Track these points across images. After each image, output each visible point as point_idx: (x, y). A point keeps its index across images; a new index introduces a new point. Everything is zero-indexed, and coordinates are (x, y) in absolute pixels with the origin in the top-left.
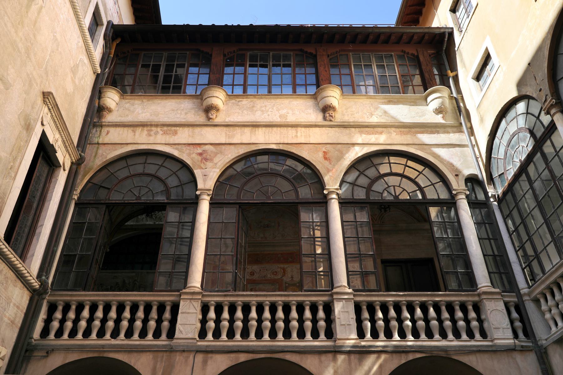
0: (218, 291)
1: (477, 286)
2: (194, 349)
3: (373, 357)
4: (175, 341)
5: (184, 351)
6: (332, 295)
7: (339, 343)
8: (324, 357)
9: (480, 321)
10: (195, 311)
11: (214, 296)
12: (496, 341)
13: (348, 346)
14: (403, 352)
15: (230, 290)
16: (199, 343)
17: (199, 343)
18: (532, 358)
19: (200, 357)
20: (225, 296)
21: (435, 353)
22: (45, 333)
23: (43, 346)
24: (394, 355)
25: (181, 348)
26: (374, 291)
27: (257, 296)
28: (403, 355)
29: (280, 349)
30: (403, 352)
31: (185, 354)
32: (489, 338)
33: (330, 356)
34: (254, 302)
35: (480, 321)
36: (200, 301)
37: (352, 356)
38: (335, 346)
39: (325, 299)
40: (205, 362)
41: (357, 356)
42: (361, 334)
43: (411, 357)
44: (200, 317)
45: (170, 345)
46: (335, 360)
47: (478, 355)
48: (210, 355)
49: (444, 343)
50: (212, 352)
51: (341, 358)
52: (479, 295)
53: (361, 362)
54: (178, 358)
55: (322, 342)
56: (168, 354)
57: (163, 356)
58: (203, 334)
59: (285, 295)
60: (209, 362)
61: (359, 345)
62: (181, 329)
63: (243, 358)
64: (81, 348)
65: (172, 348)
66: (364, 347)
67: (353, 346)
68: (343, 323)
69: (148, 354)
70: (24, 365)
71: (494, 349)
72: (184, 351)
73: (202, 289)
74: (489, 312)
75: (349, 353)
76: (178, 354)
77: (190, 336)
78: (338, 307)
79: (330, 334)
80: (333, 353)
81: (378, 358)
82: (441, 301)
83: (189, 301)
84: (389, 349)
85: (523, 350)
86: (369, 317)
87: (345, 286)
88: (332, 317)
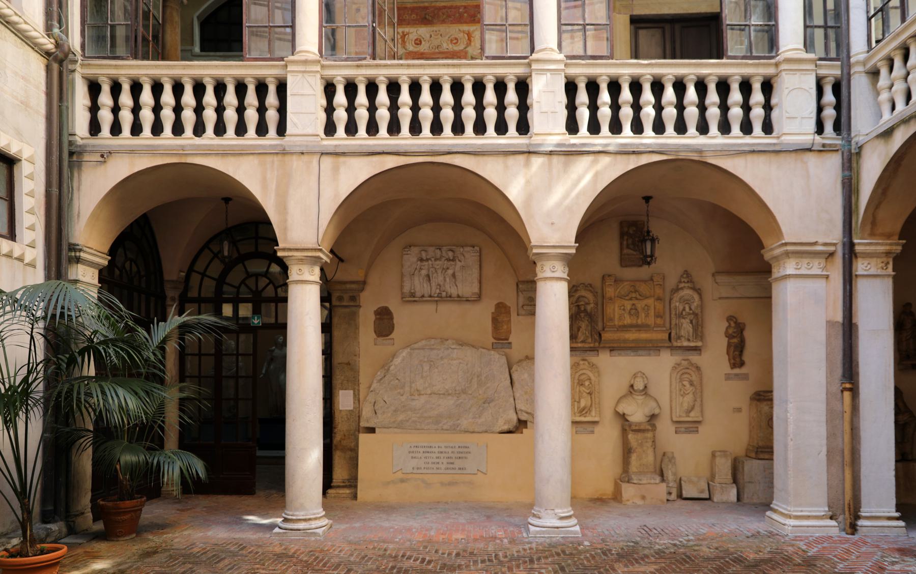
0: (346, 60)
1: (778, 49)
2: (317, 149)
3: (587, 159)
4: (287, 139)
5: (303, 153)
6: (529, 65)
7: (536, 140)
8: (511, 160)
9: (768, 107)
10: (312, 92)
11: (340, 67)
12: (783, 138)
13: (549, 145)
14: (634, 153)
15: (365, 59)
16: (325, 143)
17: (325, 143)
18: (834, 162)
19: (327, 161)
20: (358, 66)
21: (683, 155)
22: (95, 128)
23: (94, 146)
24: (619, 157)
25: (298, 149)
26: (601, 57)
27: (409, 66)
28: (633, 157)
29: (446, 149)
30: (634, 153)
31: (305, 158)
32: (774, 134)
33: (521, 158)
34: (405, 78)
35: (768, 107)
36: (319, 76)
37: (555, 159)
38: (528, 145)
39: (520, 71)
40: (336, 169)
41: (562, 158)
42: (572, 126)
43: (644, 160)
44: (324, 102)
45: (282, 145)
46: (527, 164)
47: (750, 157)
48: (342, 159)
49: (702, 140)
50: (344, 154)
52: (777, 65)
53: (566, 166)
54: (296, 163)
55: (512, 138)
56: (280, 157)
57: (273, 162)
58: (330, 129)
59: (454, 65)
60: (342, 170)
61: (567, 143)
62: (295, 120)
63: (391, 162)
64: (151, 151)
65: (284, 150)
66: (574, 145)
67: (559, 145)
68: (544, 110)
69: (251, 157)
70: (76, 174)
71: (777, 148)
72: (303, 153)
73: (321, 56)
74: (786, 91)
75: (551, 153)
76: (295, 157)
77: (310, 131)
78: (537, 87)
79: (523, 127)
80: (526, 155)
81: (594, 162)
82: (710, 75)
83: (300, 75)
84: (611, 149)
85: (825, 149)
86: (587, 102)
87: (552, 50)
88: (529, 101)
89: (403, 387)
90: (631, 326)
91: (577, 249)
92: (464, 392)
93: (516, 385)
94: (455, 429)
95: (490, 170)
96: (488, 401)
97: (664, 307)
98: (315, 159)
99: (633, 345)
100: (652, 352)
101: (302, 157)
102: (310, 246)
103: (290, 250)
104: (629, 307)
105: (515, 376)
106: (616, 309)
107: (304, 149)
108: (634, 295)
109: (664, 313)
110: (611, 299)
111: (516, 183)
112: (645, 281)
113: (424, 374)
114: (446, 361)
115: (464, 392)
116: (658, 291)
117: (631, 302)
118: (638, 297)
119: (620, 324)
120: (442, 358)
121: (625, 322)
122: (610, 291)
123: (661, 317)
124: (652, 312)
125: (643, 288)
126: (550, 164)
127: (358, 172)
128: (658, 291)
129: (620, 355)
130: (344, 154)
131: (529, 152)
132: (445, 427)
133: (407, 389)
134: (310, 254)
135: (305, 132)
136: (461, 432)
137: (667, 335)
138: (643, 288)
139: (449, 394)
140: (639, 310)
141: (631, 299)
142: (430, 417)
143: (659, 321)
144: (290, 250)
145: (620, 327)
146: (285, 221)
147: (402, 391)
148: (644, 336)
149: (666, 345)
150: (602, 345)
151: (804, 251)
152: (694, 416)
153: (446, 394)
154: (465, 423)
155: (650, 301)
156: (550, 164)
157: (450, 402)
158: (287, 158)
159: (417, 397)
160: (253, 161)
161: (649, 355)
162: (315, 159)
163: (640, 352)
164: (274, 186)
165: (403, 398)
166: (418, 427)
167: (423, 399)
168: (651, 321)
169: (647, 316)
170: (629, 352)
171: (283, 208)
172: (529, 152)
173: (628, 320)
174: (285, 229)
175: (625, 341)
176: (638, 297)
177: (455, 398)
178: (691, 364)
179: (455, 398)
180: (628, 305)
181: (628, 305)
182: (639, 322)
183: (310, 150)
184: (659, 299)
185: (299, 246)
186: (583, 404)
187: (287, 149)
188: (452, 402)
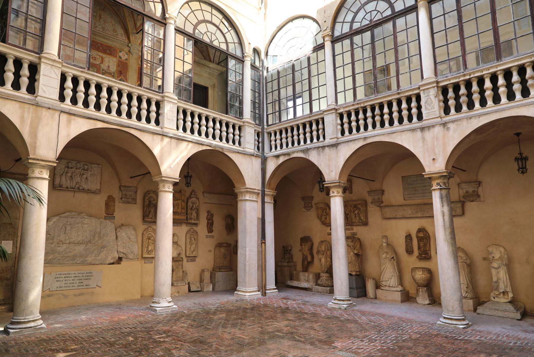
2: (59, 109)
5: (49, 108)
8: (156, 137)
19: (64, 117)
25: (46, 105)
29: (127, 125)
31: (51, 111)
33: (160, 137)
37: (173, 140)
40: (69, 122)
41: (176, 141)
46: (162, 140)
48: (73, 117)
50: (74, 115)
51: (166, 140)
53: (177, 145)
57: (29, 108)
60: (73, 122)
62: (44, 89)
63: (100, 125)
65: (37, 103)
72: (49, 108)
75: (171, 137)
76: (44, 109)
89: (53, 239)
91: (180, 180)
92: (90, 242)
93: (119, 239)
94: (83, 263)
95: (146, 139)
96: (103, 247)
98: (57, 114)
101: (49, 110)
102: (50, 159)
103: (38, 160)
105: (118, 234)
107: (51, 107)
111: (157, 146)
113: (67, 232)
114: (80, 225)
115: (90, 242)
120: (78, 223)
126: (171, 142)
127: (80, 126)
130: (74, 115)
131: (163, 135)
132: (78, 262)
133: (55, 240)
134: (50, 164)
135: (50, 97)
136: (88, 264)
139: (81, 244)
142: (69, 257)
144: (38, 160)
146: (35, 143)
147: (51, 241)
151: (251, 192)
152: (194, 254)
153: (79, 243)
154: (89, 259)
156: (171, 142)
157: (81, 248)
158: (39, 109)
159: (61, 245)
160: (16, 105)
162: (57, 114)
164: (29, 122)
165: (52, 246)
166: (62, 262)
167: (65, 246)
171: (34, 135)
172: (163, 135)
174: (35, 148)
177: (85, 246)
178: (195, 231)
179: (85, 246)
183: (54, 107)
185: (43, 159)
186: (150, 249)
187: (39, 103)
188: (82, 248)
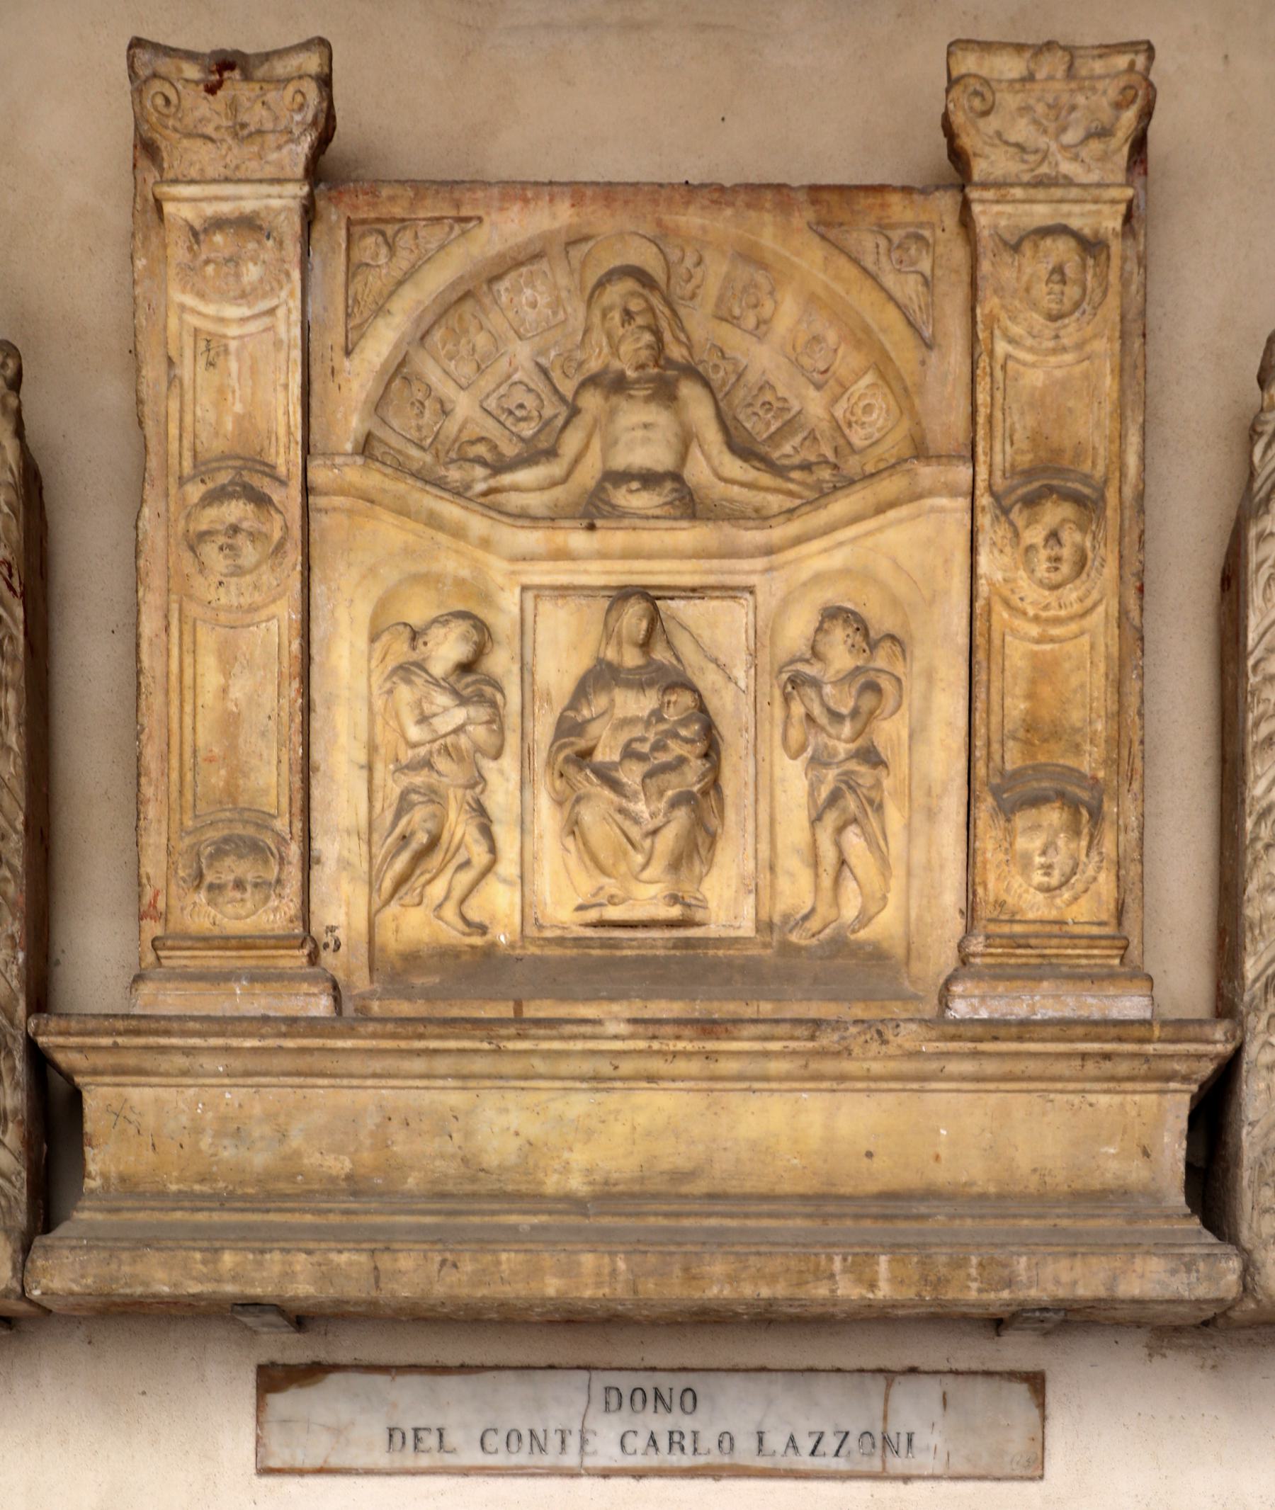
90: (599, 962)
97: (1133, 638)
99: (590, 1276)
100: (914, 1410)
104: (560, 650)
106: (346, 657)
108: (642, 437)
109: (1129, 750)
110: (245, 479)
112: (832, 205)
116: (1049, 365)
117: (597, 558)
118: (713, 466)
119: (415, 924)
121: (499, 905)
122: (239, 351)
123: (1085, 808)
124: (929, 736)
125: (788, 330)
128: (1049, 365)
129: (413, 1450)
137: (1171, 1113)
138: (788, 330)
140: (730, 704)
141: (593, 510)
143: (1042, 874)
145: (398, 969)
148: (787, 1124)
149: (1148, 1278)
150: (63, 1273)
155: (906, 548)
161: (882, 1456)
163: (734, 1411)
168: (909, 882)
169: (850, 796)
170: (561, 1405)
173: (543, 876)
175: (474, 1203)
176: (713, 466)
180: (545, 600)
181: (545, 600)
182: (726, 905)
184: (1044, 481)
